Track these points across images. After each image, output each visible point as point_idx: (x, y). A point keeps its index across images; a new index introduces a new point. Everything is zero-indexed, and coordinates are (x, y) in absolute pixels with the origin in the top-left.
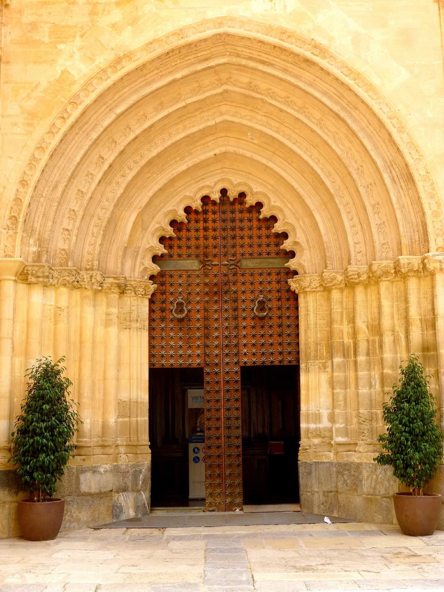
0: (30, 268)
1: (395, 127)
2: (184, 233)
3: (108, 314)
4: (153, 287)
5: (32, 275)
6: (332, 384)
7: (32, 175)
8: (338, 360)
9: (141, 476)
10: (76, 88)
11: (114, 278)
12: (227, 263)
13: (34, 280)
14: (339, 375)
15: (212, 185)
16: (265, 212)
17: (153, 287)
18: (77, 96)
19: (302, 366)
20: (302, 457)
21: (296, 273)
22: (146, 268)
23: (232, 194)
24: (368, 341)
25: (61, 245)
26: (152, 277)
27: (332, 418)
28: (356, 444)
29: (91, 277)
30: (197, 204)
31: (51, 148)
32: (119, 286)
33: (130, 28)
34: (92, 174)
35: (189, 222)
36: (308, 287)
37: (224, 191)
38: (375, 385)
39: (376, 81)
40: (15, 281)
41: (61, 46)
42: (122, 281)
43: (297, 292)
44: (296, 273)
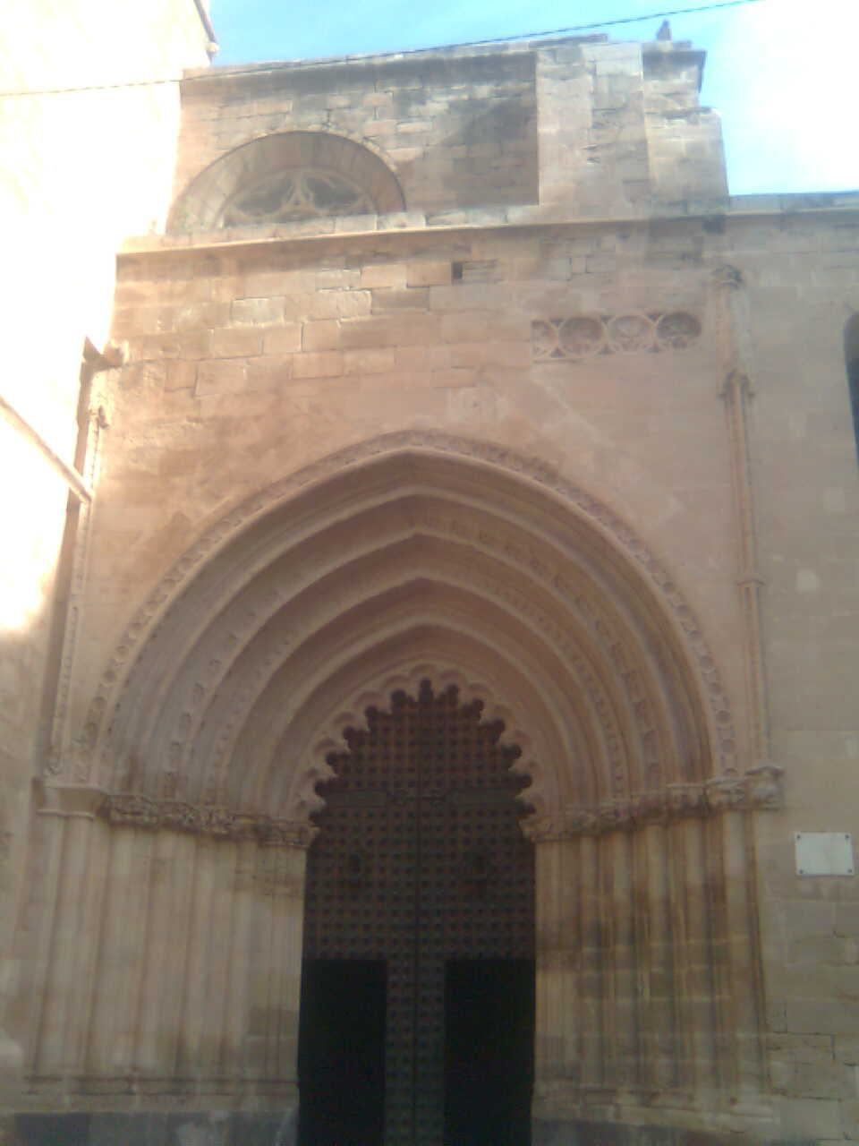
0: (113, 800)
1: (659, 584)
2: (366, 750)
3: (238, 872)
4: (313, 831)
5: (118, 810)
6: (580, 988)
7: (122, 664)
8: (588, 950)
9: (279, 1134)
10: (192, 538)
11: (251, 817)
12: (428, 795)
13: (117, 817)
14: (590, 973)
15: (407, 674)
16: (487, 715)
17: (313, 831)
18: (192, 550)
19: (539, 960)
20: (536, 1112)
21: (532, 810)
22: (303, 804)
23: (439, 688)
24: (632, 920)
25: (167, 767)
26: (315, 817)
27: (581, 1050)
28: (613, 1092)
29: (211, 815)
30: (385, 704)
31: (152, 623)
32: (256, 830)
33: (273, 451)
34: (217, 662)
35: (374, 730)
36: (549, 833)
37: (426, 686)
38: (642, 992)
39: (630, 516)
40: (91, 819)
41: (177, 481)
42: (261, 822)
43: (533, 839)
44: (532, 810)
